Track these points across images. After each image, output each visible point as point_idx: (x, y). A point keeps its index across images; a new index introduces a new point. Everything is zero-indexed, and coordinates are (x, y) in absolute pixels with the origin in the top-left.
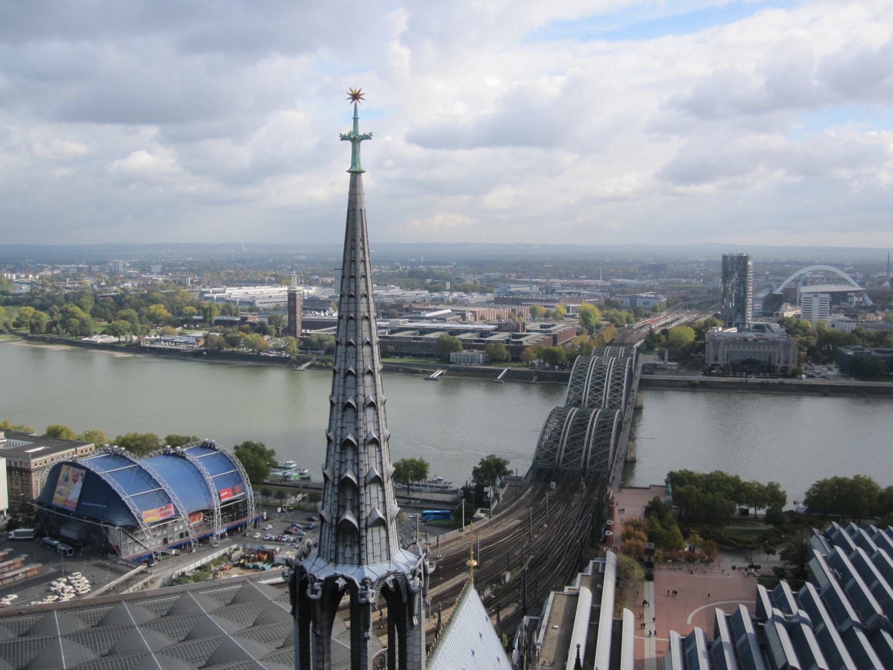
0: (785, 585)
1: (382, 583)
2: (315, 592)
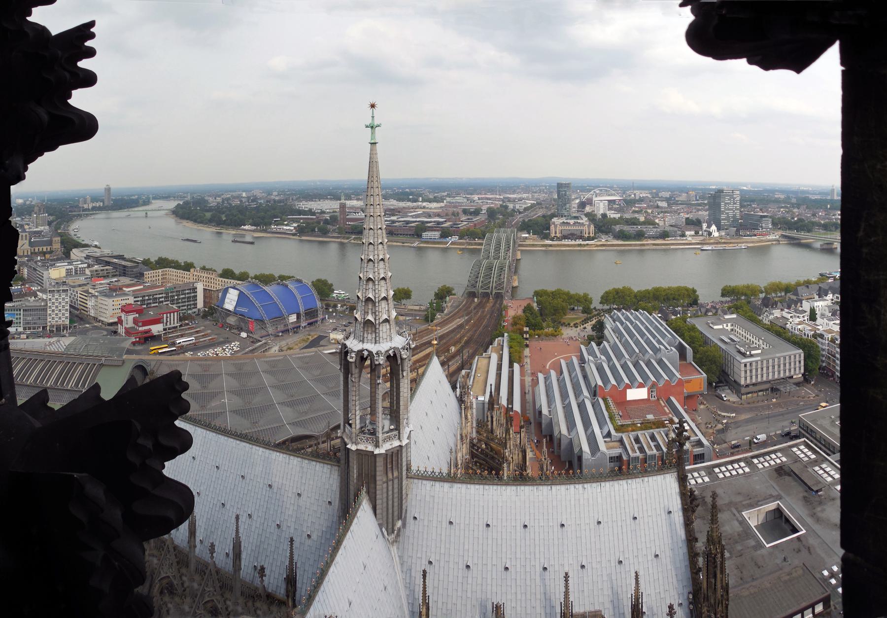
0: (593, 344)
2: (352, 358)
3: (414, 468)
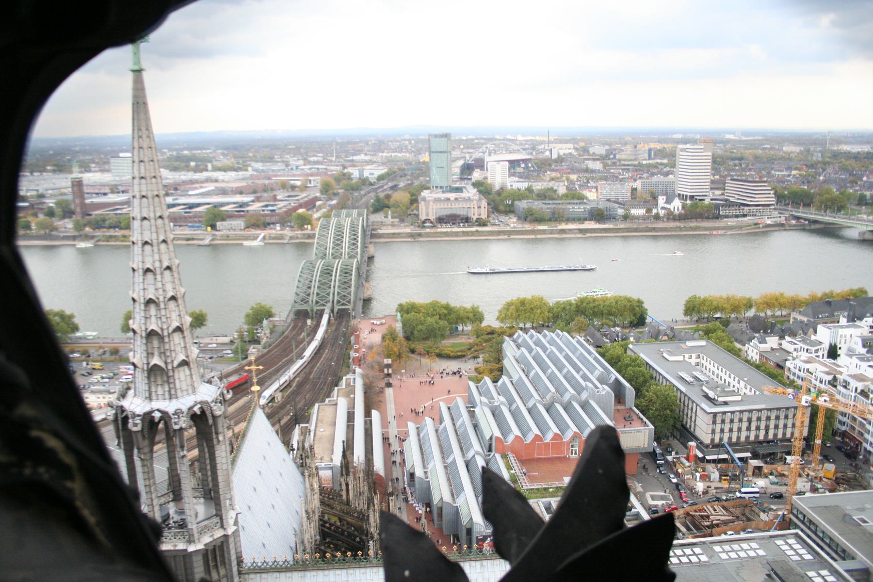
0: (487, 380)
1: (191, 412)
2: (136, 425)
3: (248, 560)
